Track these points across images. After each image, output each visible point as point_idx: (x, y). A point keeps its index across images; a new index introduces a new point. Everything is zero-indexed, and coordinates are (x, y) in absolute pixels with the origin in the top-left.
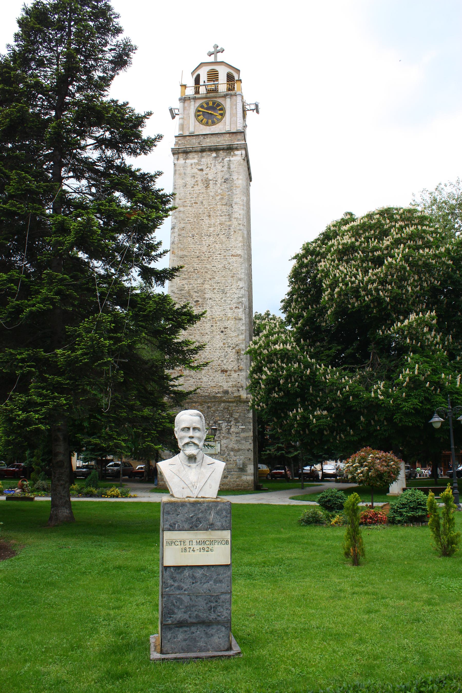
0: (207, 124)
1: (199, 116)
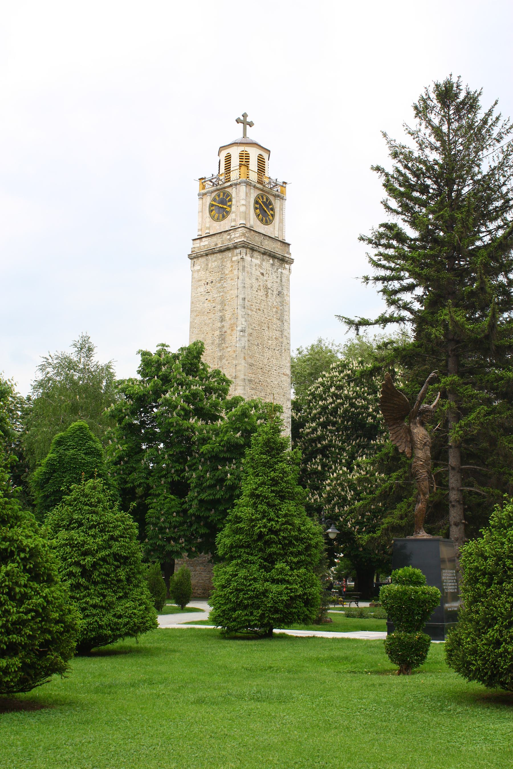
0: (218, 220)
1: (212, 211)
